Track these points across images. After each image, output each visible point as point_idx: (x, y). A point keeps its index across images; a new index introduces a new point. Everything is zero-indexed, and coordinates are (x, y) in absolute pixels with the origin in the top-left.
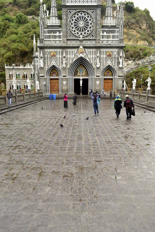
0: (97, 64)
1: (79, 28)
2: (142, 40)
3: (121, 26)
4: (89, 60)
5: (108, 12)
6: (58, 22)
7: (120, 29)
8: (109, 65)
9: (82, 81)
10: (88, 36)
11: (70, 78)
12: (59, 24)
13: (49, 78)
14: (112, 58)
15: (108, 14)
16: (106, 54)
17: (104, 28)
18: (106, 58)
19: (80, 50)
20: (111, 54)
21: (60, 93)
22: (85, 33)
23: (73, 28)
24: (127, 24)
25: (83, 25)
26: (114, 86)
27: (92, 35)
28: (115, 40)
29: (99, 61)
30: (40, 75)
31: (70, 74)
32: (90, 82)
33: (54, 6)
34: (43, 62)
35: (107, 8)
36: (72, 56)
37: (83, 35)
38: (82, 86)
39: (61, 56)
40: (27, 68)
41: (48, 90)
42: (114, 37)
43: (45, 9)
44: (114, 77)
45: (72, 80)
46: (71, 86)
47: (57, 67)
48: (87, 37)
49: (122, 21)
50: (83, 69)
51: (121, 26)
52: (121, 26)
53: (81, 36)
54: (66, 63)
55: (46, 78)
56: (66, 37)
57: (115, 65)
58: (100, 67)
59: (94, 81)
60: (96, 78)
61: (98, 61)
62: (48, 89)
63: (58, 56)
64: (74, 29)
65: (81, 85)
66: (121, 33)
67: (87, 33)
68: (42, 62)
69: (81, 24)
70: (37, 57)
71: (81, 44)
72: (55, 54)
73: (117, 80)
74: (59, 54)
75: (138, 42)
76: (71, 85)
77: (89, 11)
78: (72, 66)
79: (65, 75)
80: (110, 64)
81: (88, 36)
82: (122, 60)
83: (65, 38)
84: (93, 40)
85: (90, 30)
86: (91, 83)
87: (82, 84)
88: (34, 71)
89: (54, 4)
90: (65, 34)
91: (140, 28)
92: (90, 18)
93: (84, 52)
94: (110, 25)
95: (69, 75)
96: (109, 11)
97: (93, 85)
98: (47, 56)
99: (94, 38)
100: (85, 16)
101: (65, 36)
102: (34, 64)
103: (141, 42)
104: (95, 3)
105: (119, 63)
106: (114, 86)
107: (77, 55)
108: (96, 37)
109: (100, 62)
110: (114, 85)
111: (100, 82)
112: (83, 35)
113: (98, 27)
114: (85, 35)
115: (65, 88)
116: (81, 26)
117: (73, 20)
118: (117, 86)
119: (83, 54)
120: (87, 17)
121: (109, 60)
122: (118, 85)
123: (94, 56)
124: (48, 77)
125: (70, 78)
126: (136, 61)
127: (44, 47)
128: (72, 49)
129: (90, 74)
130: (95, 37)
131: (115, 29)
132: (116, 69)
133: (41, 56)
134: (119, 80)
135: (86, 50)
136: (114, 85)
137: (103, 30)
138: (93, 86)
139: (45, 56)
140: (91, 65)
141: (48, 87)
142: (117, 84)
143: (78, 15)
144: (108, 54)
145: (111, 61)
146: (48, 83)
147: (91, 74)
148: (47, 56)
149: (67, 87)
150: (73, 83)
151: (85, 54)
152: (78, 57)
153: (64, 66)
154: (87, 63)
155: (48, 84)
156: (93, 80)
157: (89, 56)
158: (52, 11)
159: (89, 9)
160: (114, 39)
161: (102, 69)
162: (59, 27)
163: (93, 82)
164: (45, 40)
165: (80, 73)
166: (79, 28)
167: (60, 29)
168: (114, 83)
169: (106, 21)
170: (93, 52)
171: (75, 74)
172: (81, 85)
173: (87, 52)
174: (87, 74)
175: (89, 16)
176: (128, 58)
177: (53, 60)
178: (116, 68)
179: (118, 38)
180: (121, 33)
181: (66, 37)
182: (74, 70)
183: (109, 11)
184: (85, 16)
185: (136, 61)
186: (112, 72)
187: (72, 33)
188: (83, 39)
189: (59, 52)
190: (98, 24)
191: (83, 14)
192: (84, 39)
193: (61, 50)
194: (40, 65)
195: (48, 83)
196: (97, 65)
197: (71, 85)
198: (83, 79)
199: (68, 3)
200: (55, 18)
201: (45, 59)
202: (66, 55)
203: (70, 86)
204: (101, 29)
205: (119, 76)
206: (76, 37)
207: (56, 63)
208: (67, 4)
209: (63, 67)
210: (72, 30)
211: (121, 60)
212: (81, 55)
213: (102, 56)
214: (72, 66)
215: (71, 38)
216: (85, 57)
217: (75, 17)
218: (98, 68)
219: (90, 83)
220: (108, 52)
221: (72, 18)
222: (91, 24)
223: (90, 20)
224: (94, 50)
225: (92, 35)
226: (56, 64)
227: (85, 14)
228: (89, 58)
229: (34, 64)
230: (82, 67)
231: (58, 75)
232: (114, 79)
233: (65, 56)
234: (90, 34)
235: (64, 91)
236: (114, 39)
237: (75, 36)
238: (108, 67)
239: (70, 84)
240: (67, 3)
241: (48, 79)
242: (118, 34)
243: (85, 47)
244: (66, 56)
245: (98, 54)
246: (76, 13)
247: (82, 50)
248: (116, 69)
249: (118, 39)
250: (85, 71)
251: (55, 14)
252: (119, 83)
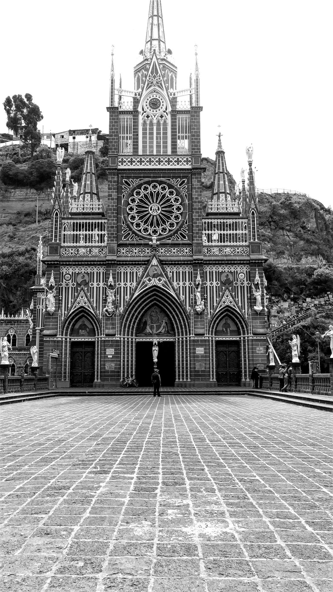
0: (196, 303)
1: (148, 219)
2: (312, 255)
3: (253, 213)
4: (176, 294)
5: (219, 184)
6: (97, 206)
7: (249, 220)
8: (228, 306)
9: (157, 348)
10: (171, 236)
11: (124, 342)
12: (101, 211)
13: (68, 340)
14: (235, 289)
15: (218, 187)
16: (218, 279)
17: (211, 219)
18: (219, 289)
19: (151, 270)
20: (231, 277)
21: (96, 381)
22: (164, 230)
23: (133, 218)
24: (270, 220)
26: (245, 361)
27: (181, 234)
28: (240, 246)
29: (201, 296)
30: (46, 332)
31: (124, 331)
32: (179, 349)
33: (88, 171)
34: (55, 300)
35: (217, 175)
36: (131, 284)
37: (160, 234)
38: (157, 363)
39: (101, 284)
40: (18, 321)
41: (65, 373)
42: (235, 238)
43: (68, 179)
44: (244, 338)
45: (132, 346)
46: (128, 361)
47: (92, 311)
49: (253, 202)
50: (160, 316)
51: (253, 212)
52: (253, 212)
53: (154, 237)
54: (114, 303)
55: (60, 339)
56: (118, 238)
57: (243, 307)
58: (204, 310)
59: (188, 347)
60: (194, 341)
61: (198, 294)
62: (65, 369)
63: (95, 284)
64: (136, 220)
65: (155, 360)
66: (254, 228)
67: (170, 231)
68: (53, 300)
69: (155, 209)
70: (42, 291)
71: (154, 255)
72: (87, 278)
73: (252, 345)
74: (98, 280)
75: (301, 259)
76: (128, 358)
77: (173, 182)
78: (132, 309)
79: (111, 332)
80: (231, 302)
82: (260, 293)
83: (113, 240)
84: (184, 245)
85: (177, 223)
86: (183, 353)
87: (158, 357)
88: (34, 325)
89: (89, 168)
90: (114, 231)
91: (304, 228)
92: (176, 195)
93: (161, 275)
94: (224, 211)
95: (122, 333)
96: (222, 182)
97: (187, 357)
98: (67, 285)
99: (186, 241)
100: (164, 192)
101: (114, 237)
102: (35, 308)
103: (309, 258)
104: (187, 164)
105: (252, 301)
106: (245, 361)
107: (144, 283)
108: (191, 238)
109: (203, 298)
110: (245, 357)
111: (205, 349)
112: (160, 234)
113: (195, 216)
114: (165, 234)
115: (110, 366)
117: (133, 201)
118: (253, 360)
119: (160, 280)
120: (167, 194)
121: (227, 292)
122: (256, 356)
123: (187, 284)
124: (66, 339)
125: (124, 342)
126: (301, 303)
127: (60, 262)
128: (131, 266)
129: (178, 329)
130: (189, 239)
131: (237, 221)
132: (246, 316)
133: (50, 285)
134: (258, 345)
135: (168, 269)
136: (245, 357)
137: (208, 222)
138: (187, 361)
139: (61, 285)
140: (181, 306)
141: (65, 365)
142: (253, 356)
143: (146, 189)
144: (223, 278)
145: (231, 295)
146: (66, 354)
147: (182, 328)
148: (67, 285)
149: (116, 365)
150: (132, 354)
151: (164, 279)
152: (146, 285)
153: (110, 308)
154: (169, 302)
155: (66, 357)
156: (186, 346)
157: (175, 283)
158: (86, 181)
160: (238, 244)
161: (209, 316)
162: (101, 216)
163: (187, 349)
164: (64, 247)
165: (152, 328)
166: (148, 219)
167: (103, 221)
168: (245, 353)
169: (214, 202)
170: (184, 273)
171: (140, 330)
172: (155, 360)
173: (170, 275)
174: (171, 330)
175: (173, 192)
176: (279, 296)
177: (82, 293)
178: (246, 312)
179: (246, 241)
180: (254, 228)
181: (118, 238)
182: (136, 319)
183: (222, 182)
184: (164, 192)
185: (301, 303)
186: (236, 324)
187: (131, 229)
188: (158, 242)
189: (98, 274)
190: (196, 209)
191: (159, 188)
192: (161, 244)
193: (102, 270)
194: (46, 308)
195: (66, 354)
196: (196, 307)
197: (128, 358)
198: (160, 344)
199: (122, 164)
200: (92, 198)
201: (59, 291)
202: (115, 282)
203: (124, 361)
204: (204, 221)
205: (255, 334)
207: (88, 300)
208: (121, 167)
209: (107, 311)
210: (132, 223)
211: (258, 295)
212: (155, 282)
213: (208, 283)
214: (132, 309)
215: (130, 241)
216: (163, 285)
217: (138, 193)
218: (199, 315)
219: (179, 353)
220: (225, 274)
221: (133, 196)
222: (178, 209)
223: (176, 200)
224: (187, 269)
225: (181, 234)
226: (88, 304)
227: (164, 189)
228: (176, 288)
229: (35, 308)
230: (158, 310)
231: (92, 333)
232: (244, 341)
233: (113, 284)
234: (176, 232)
235: (108, 376)
236: (238, 244)
237: (138, 236)
238: (225, 311)
239: (124, 358)
240: (120, 164)
241: (66, 342)
242: (247, 232)
243: (162, 263)
244: (115, 285)
245: (199, 278)
246: (141, 185)
247: (156, 268)
248: (246, 316)
249: (247, 244)
250: (166, 323)
251: (91, 188)
252: (257, 352)
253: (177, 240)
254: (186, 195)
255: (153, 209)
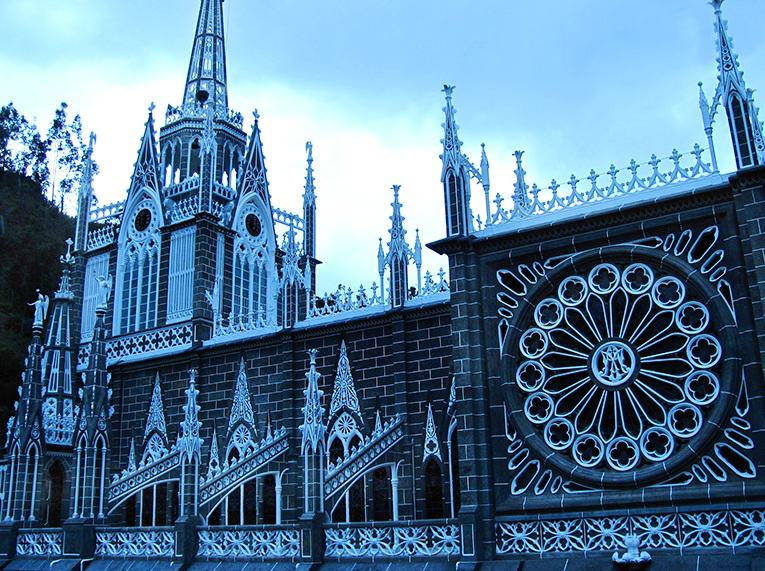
10: (686, 464)
25: (631, 370)
48: (676, 472)
81: (686, 464)
116: (614, 382)
159: (662, 231)
187: (535, 454)
206: (580, 482)
225: (724, 451)
227: (637, 279)
234: (705, 447)
237: (566, 476)
253: (711, 479)
254: (725, 289)
255: (605, 362)
